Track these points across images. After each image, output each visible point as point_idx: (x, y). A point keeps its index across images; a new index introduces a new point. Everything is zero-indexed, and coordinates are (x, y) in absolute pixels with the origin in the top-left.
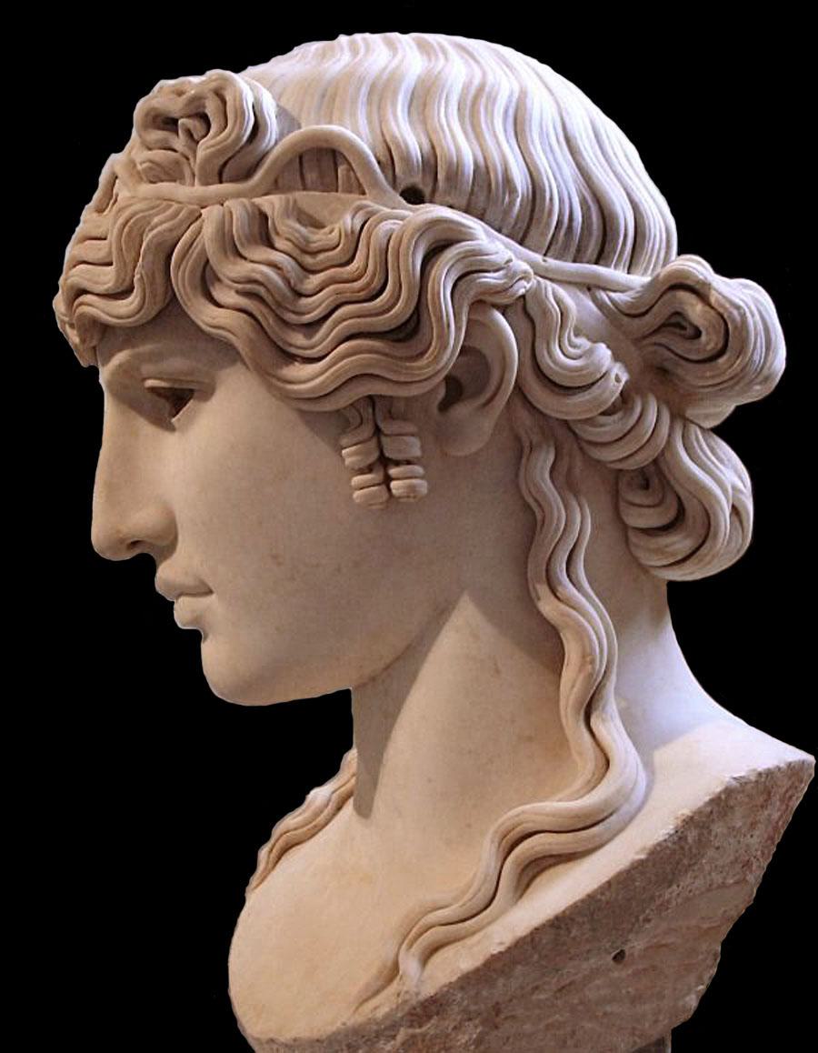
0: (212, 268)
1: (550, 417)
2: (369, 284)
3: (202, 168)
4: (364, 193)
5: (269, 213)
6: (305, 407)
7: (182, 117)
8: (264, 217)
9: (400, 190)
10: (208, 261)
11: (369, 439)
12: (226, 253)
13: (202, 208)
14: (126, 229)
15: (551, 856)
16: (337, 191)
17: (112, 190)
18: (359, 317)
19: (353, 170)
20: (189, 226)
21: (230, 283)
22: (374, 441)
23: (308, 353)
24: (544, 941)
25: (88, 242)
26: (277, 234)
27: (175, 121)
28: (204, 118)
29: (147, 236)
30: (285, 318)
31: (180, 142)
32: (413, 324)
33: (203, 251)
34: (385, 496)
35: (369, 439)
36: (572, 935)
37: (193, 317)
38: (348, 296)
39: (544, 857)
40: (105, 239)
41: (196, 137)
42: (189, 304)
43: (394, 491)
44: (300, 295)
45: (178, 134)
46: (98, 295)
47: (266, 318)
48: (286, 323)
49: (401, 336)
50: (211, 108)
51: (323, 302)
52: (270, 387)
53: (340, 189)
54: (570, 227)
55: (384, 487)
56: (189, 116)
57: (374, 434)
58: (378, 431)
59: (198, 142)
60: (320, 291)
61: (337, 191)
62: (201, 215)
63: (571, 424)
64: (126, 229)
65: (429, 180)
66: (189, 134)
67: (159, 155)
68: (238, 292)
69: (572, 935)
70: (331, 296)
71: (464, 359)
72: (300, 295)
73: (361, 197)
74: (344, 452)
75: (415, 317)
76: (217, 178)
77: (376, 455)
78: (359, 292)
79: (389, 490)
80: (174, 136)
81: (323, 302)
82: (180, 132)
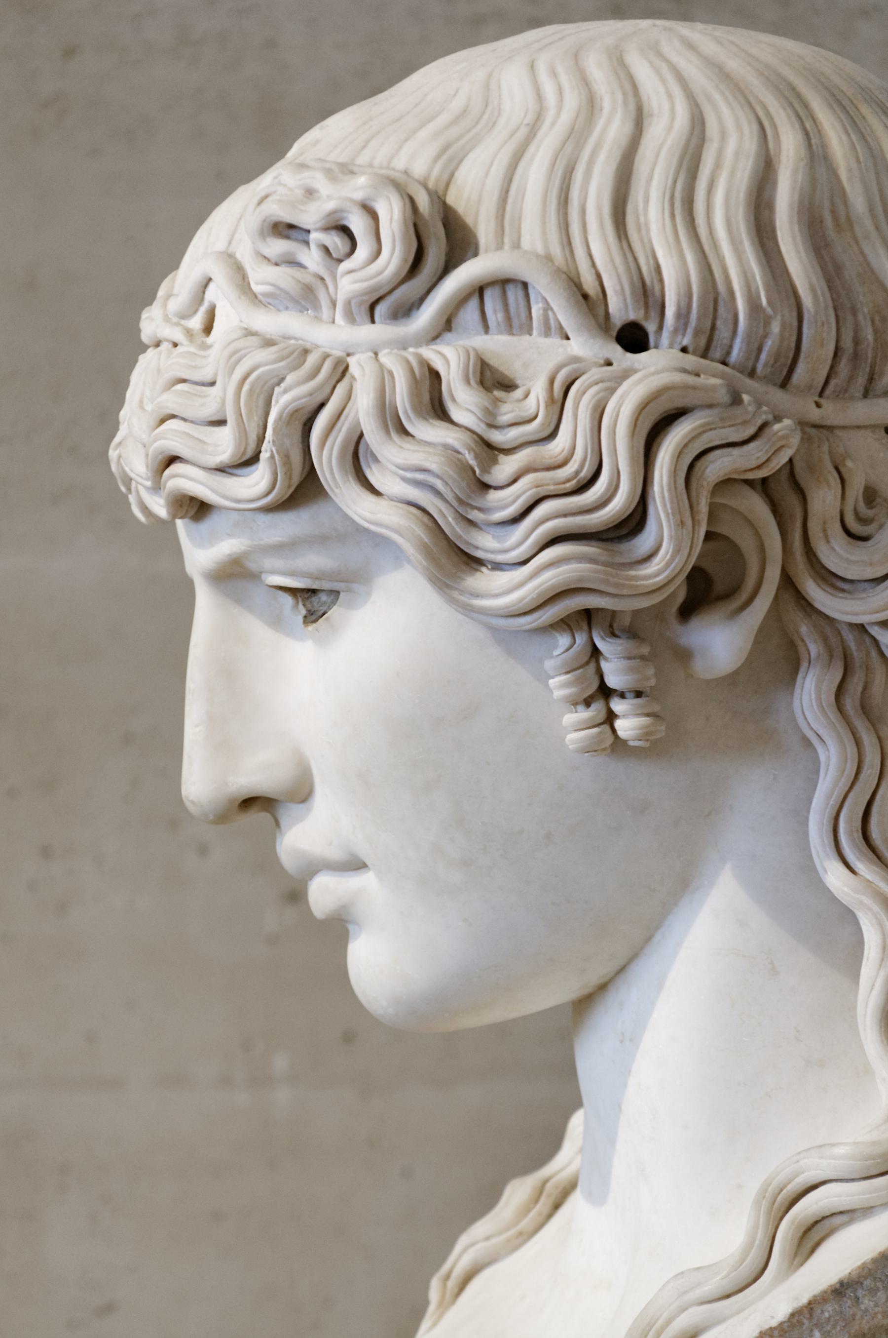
0: (367, 446)
1: (834, 619)
2: (577, 473)
3: (348, 303)
4: (568, 338)
5: (439, 366)
6: (496, 622)
7: (316, 230)
8: (435, 376)
9: (614, 334)
10: (361, 435)
11: (588, 663)
12: (388, 432)
13: (348, 355)
14: (246, 387)
15: (841, 1213)
16: (531, 334)
17: (204, 292)
18: (565, 516)
19: (552, 309)
20: (334, 387)
21: (393, 468)
22: (592, 667)
23: (500, 558)
24: (826, 1315)
25: (180, 387)
26: (454, 400)
27: (309, 231)
28: (345, 231)
29: (277, 402)
30: (470, 517)
31: (312, 259)
32: (637, 517)
33: (357, 424)
34: (610, 739)
35: (588, 663)
36: (863, 1307)
37: (344, 508)
38: (552, 489)
39: (833, 1215)
40: (213, 384)
41: (334, 255)
42: (337, 491)
43: (620, 733)
44: (486, 487)
45: (310, 249)
46: (204, 468)
47: (445, 517)
48: (471, 523)
49: (624, 532)
50: (357, 224)
51: (518, 497)
52: (453, 601)
53: (535, 332)
54: (856, 357)
55: (606, 727)
56: (326, 229)
57: (592, 656)
58: (596, 652)
59: (340, 261)
60: (515, 481)
61: (531, 334)
62: (347, 368)
63: (867, 627)
64: (246, 387)
65: (654, 315)
66: (326, 250)
67: (282, 276)
68: (404, 479)
69: (863, 1307)
70: (530, 489)
71: (712, 545)
72: (486, 487)
73: (565, 342)
74: (551, 681)
75: (641, 508)
76: (368, 319)
77: (595, 685)
78: (564, 483)
79: (614, 731)
80: (305, 249)
81: (518, 497)
82: (312, 245)
